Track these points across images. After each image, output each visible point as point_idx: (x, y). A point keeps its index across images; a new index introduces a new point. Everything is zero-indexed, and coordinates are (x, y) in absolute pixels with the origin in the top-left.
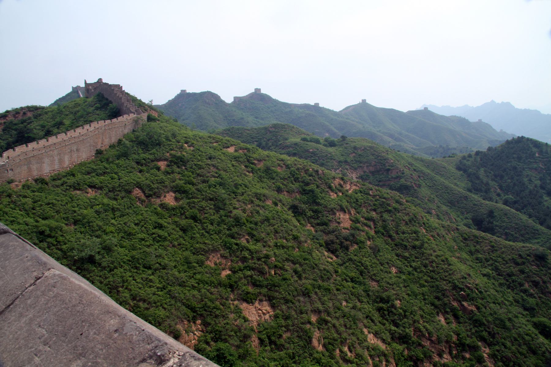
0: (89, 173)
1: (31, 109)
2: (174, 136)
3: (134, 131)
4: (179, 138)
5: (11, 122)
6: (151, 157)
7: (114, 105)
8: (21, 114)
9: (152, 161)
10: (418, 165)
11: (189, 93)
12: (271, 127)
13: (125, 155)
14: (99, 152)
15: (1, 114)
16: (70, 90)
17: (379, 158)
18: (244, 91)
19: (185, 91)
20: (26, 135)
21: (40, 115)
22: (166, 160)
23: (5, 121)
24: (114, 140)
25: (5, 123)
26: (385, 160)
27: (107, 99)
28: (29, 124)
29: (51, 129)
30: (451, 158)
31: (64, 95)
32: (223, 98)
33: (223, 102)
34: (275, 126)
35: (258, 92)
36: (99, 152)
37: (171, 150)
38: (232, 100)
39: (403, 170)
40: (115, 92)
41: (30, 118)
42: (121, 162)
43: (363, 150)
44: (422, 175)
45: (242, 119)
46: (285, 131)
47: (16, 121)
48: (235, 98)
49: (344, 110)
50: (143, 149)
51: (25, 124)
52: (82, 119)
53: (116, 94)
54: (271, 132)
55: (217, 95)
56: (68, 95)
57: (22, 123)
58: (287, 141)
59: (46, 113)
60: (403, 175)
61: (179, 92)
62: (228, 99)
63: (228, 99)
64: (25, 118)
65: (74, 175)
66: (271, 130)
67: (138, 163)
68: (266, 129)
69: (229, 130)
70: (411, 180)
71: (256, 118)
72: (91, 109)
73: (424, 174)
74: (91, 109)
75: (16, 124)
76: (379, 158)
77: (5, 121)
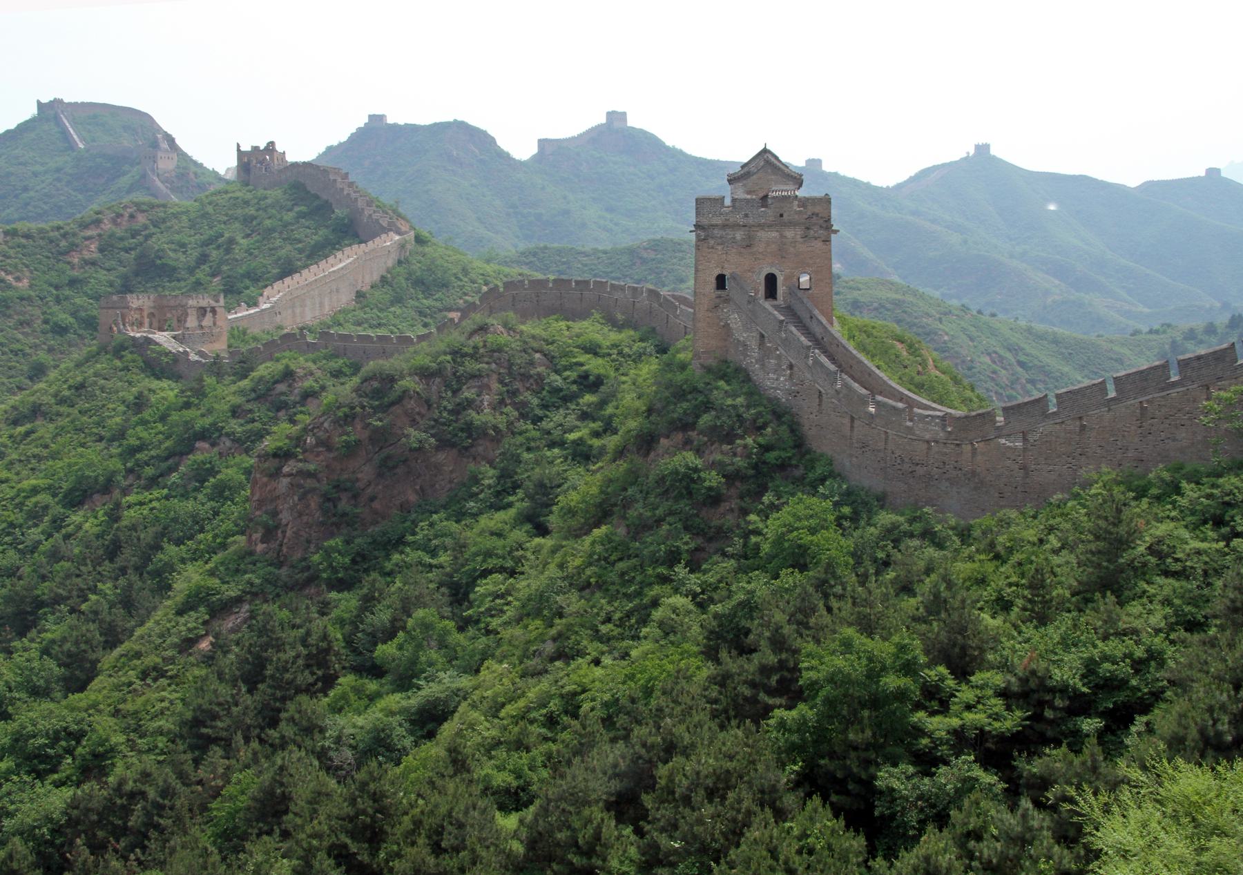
0: (359, 324)
1: (145, 207)
2: (465, 271)
3: (400, 262)
4: (473, 275)
5: (112, 236)
6: (438, 304)
7: (339, 212)
8: (126, 218)
9: (440, 311)
10: (1034, 352)
11: (395, 126)
12: (646, 249)
13: (398, 300)
14: (360, 295)
15: (95, 216)
16: (31, 111)
17: (915, 329)
18: (573, 121)
19: (381, 118)
20: (158, 262)
21: (164, 221)
22: (458, 310)
23: (99, 231)
24: (376, 277)
25: (100, 235)
26: (928, 334)
27: (317, 197)
28: (148, 237)
29: (207, 250)
30: (1154, 337)
31: (12, 126)
32: (504, 143)
33: (504, 157)
34: (656, 246)
35: (617, 125)
36: (360, 295)
37: (466, 294)
38: (533, 150)
39: (972, 361)
40: (339, 186)
41: (146, 227)
42: (396, 309)
43: (876, 309)
44: (1041, 377)
45: (566, 213)
46: (682, 259)
47: (119, 232)
48: (542, 143)
49: (912, 180)
50: (423, 292)
51: (140, 238)
52: (276, 235)
53: (342, 190)
54: (644, 261)
55: (484, 133)
56: (24, 128)
57: (133, 237)
58: (683, 286)
59: (175, 216)
60: (969, 373)
61: (362, 121)
62: (520, 145)
63: (520, 145)
64: (136, 226)
65: (340, 324)
66: (645, 255)
67: (421, 313)
68: (631, 251)
69: (535, 254)
70: (990, 385)
71: (610, 210)
72: (288, 217)
73: (1047, 374)
74: (288, 217)
75: (122, 239)
76: (915, 329)
77: (99, 231)
